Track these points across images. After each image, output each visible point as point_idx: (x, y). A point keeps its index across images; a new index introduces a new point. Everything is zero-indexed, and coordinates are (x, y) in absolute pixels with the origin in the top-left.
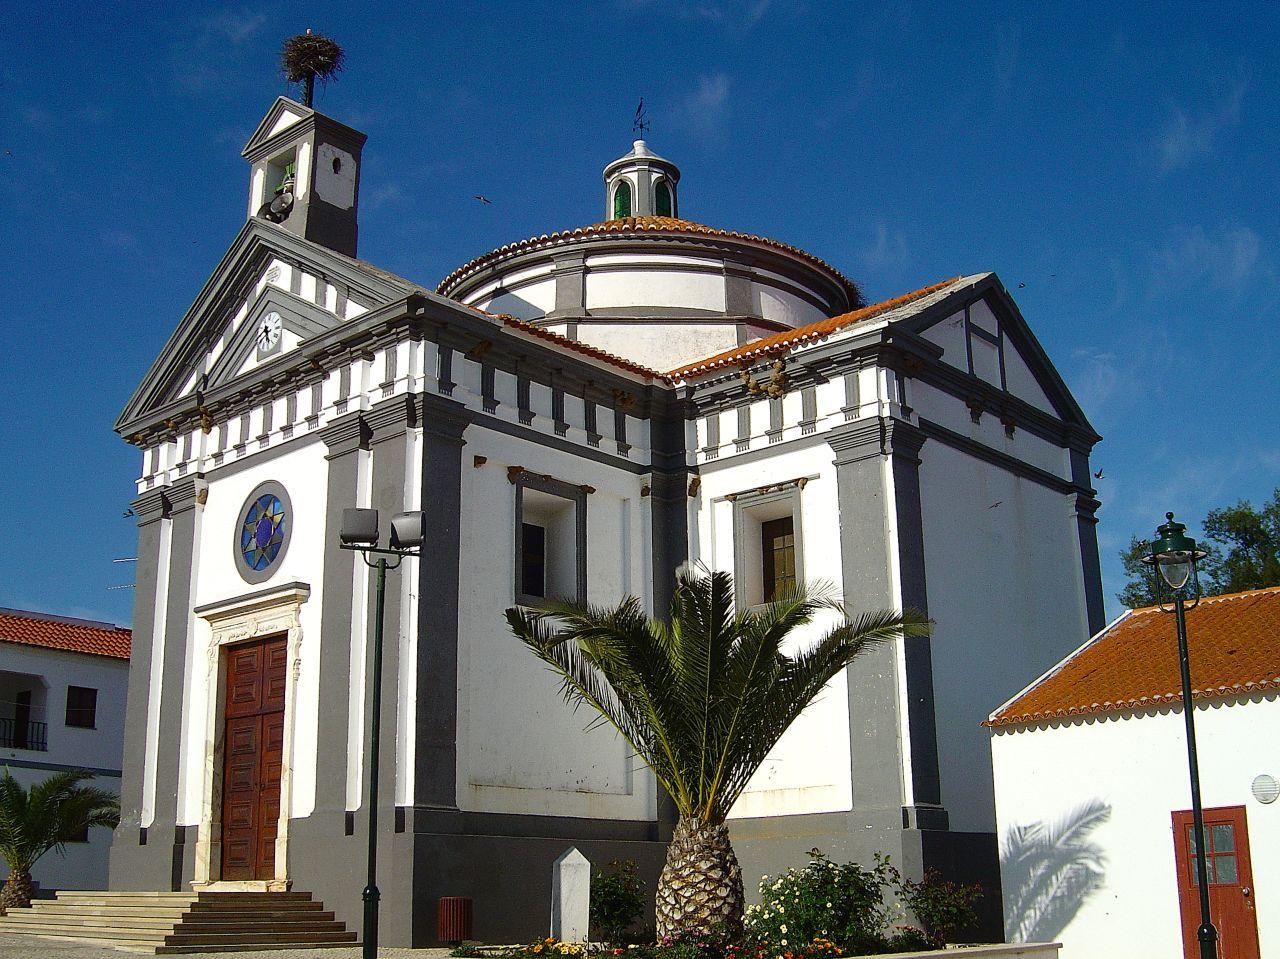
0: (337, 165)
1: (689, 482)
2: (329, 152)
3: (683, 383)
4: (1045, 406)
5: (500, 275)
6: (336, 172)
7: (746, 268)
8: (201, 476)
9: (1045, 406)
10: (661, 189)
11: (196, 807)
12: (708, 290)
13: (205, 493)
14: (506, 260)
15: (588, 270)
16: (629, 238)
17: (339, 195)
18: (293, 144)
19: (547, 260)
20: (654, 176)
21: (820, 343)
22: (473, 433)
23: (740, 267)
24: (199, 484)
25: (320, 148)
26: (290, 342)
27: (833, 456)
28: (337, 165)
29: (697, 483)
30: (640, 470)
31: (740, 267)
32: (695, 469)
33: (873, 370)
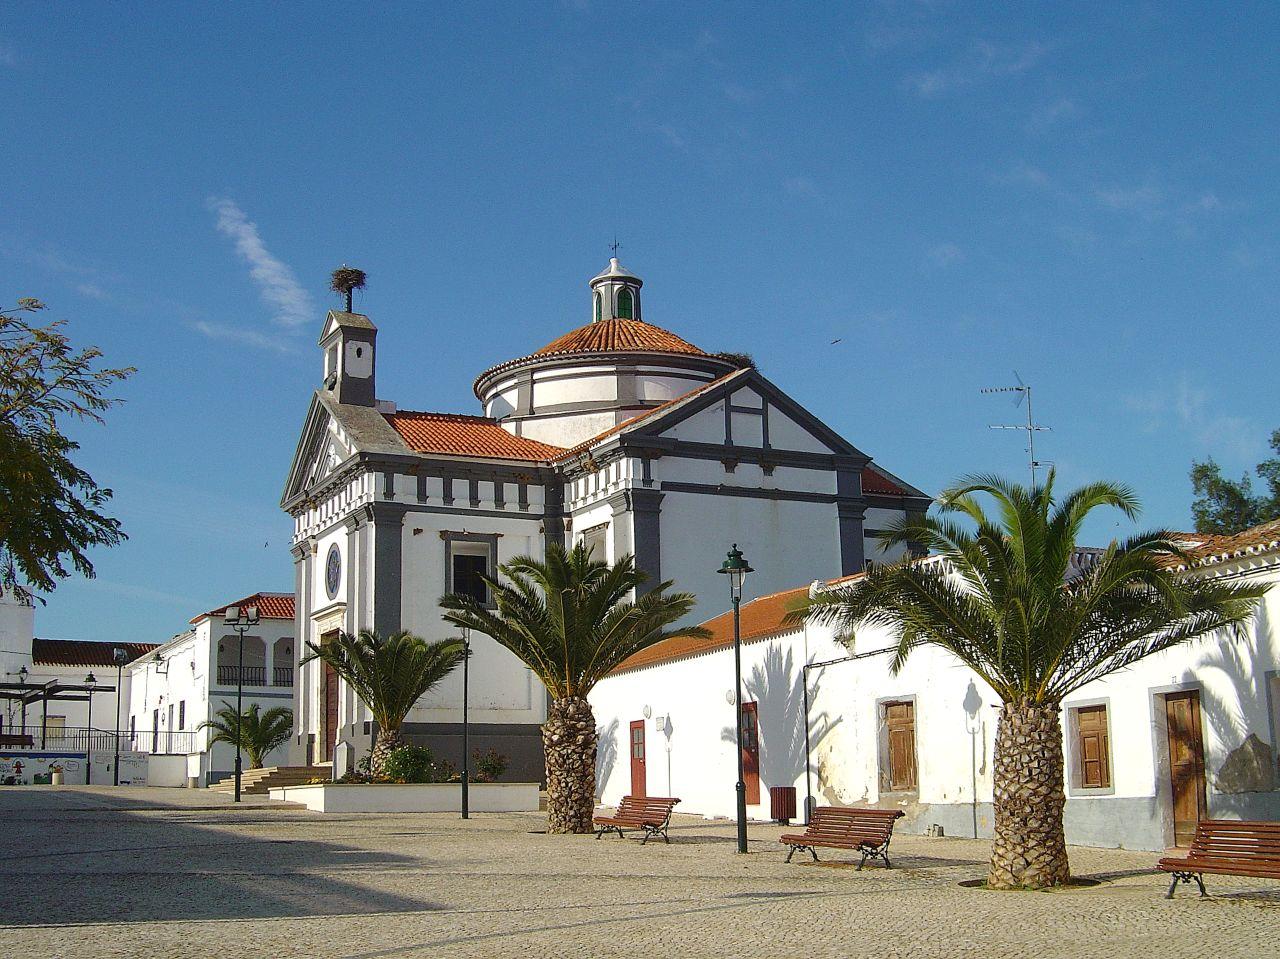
0: (359, 352)
1: (565, 523)
2: (353, 345)
3: (555, 465)
4: (821, 448)
5: (495, 385)
6: (359, 356)
7: (631, 368)
8: (314, 537)
9: (821, 448)
10: (623, 295)
11: (315, 728)
12: (603, 387)
13: (316, 546)
14: (494, 376)
15: (534, 382)
16: (561, 359)
17: (359, 370)
18: (334, 343)
19: (512, 376)
20: (616, 288)
21: (599, 445)
22: (411, 520)
23: (626, 368)
24: (312, 542)
25: (347, 345)
26: (339, 461)
27: (611, 511)
28: (359, 352)
29: (570, 523)
30: (536, 517)
31: (626, 368)
32: (569, 515)
33: (625, 460)
